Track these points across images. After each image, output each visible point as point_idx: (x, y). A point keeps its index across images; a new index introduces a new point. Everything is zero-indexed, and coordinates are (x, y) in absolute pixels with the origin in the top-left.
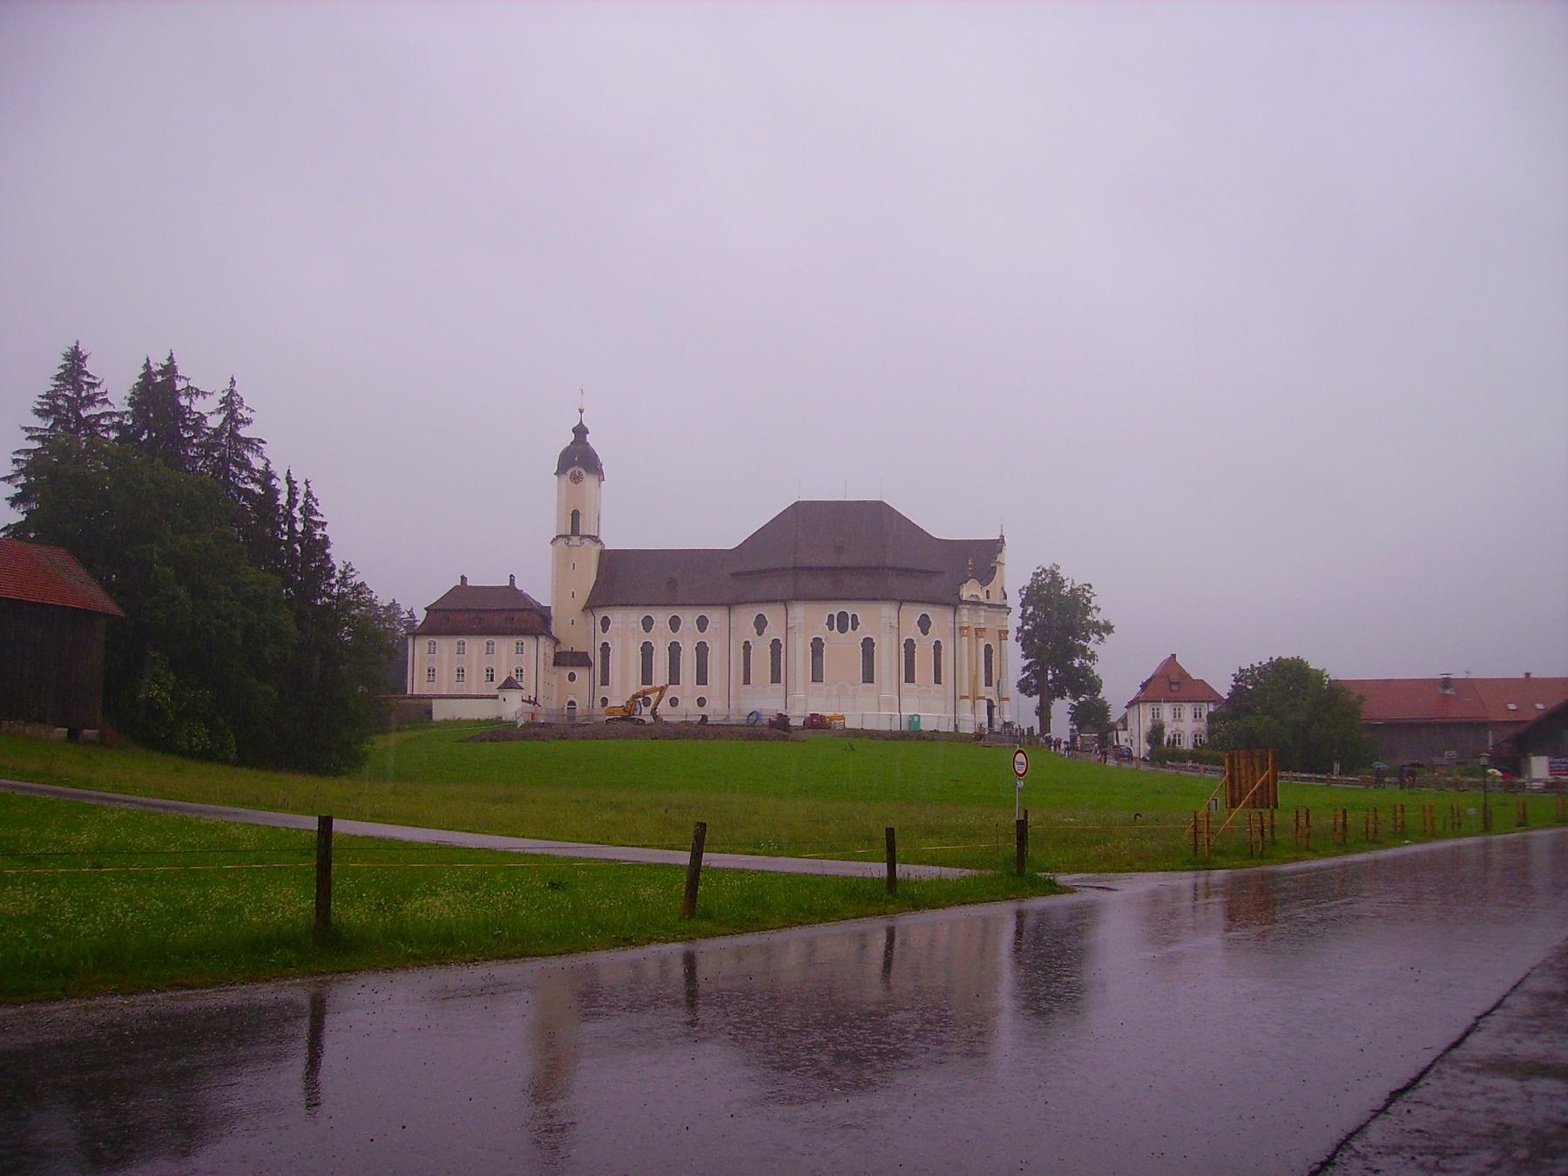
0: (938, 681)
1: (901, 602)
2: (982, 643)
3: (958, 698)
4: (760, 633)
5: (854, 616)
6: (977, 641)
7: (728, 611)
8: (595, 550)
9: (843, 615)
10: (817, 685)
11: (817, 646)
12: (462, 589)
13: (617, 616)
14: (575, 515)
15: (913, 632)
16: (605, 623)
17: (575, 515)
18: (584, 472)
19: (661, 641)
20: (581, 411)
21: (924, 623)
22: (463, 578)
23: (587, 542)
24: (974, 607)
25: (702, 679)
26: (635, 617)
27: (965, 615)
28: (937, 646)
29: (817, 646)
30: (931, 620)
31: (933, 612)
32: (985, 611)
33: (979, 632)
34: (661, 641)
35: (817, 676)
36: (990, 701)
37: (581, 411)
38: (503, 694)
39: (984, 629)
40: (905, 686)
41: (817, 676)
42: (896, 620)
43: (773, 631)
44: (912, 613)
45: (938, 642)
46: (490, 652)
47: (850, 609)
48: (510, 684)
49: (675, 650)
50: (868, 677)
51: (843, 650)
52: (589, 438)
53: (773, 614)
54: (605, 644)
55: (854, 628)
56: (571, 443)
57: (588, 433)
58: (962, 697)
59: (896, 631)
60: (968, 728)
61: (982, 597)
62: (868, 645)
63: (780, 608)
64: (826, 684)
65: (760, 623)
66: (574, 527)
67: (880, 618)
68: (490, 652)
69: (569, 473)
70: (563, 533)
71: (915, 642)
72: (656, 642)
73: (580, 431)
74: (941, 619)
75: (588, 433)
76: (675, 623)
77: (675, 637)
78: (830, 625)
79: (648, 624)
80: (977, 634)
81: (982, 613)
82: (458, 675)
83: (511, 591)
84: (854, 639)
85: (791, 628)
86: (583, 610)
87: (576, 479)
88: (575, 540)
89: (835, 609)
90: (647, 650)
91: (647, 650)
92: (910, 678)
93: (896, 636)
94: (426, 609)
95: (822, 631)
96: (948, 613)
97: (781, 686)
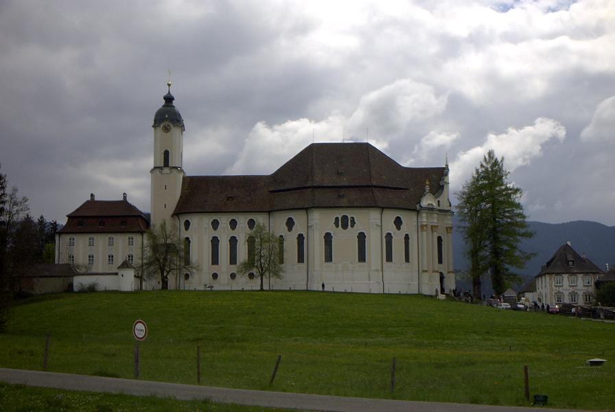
0: (407, 260)
1: (383, 208)
2: (436, 235)
3: (421, 271)
4: (290, 229)
6: (432, 235)
7: (268, 219)
8: (181, 176)
9: (345, 218)
11: (328, 238)
12: (92, 203)
13: (195, 220)
14: (166, 154)
15: (390, 227)
16: (187, 224)
17: (166, 154)
18: (172, 126)
19: (224, 235)
20: (169, 85)
21: (398, 222)
22: (92, 195)
23: (174, 171)
24: (430, 212)
26: (206, 220)
27: (424, 218)
28: (407, 237)
29: (328, 238)
30: (402, 220)
31: (404, 216)
32: (438, 214)
33: (433, 228)
34: (224, 235)
35: (329, 258)
36: (441, 274)
38: (121, 272)
39: (437, 226)
40: (386, 264)
41: (329, 258)
43: (299, 228)
44: (390, 216)
45: (407, 235)
46: (111, 244)
47: (350, 214)
48: (125, 265)
49: (233, 241)
50: (362, 258)
51: (345, 241)
53: (299, 218)
54: (187, 239)
55: (352, 226)
56: (163, 106)
57: (173, 99)
58: (424, 271)
59: (379, 228)
60: (426, 290)
61: (435, 205)
62: (362, 237)
63: (303, 212)
65: (290, 224)
66: (166, 161)
67: (369, 219)
68: (111, 244)
69: (162, 126)
70: (158, 165)
71: (392, 235)
72: (238, 236)
73: (169, 99)
74: (409, 220)
75: (173, 99)
76: (233, 224)
77: (233, 233)
79: (215, 224)
80: (432, 229)
81: (435, 216)
82: (90, 260)
83: (124, 204)
84: (351, 235)
85: (311, 226)
86: (172, 216)
87: (167, 129)
88: (166, 170)
89: (340, 214)
90: (215, 242)
91: (215, 242)
92: (389, 258)
93: (379, 231)
94: (67, 216)
95: (331, 228)
96: (413, 216)
97: (304, 265)
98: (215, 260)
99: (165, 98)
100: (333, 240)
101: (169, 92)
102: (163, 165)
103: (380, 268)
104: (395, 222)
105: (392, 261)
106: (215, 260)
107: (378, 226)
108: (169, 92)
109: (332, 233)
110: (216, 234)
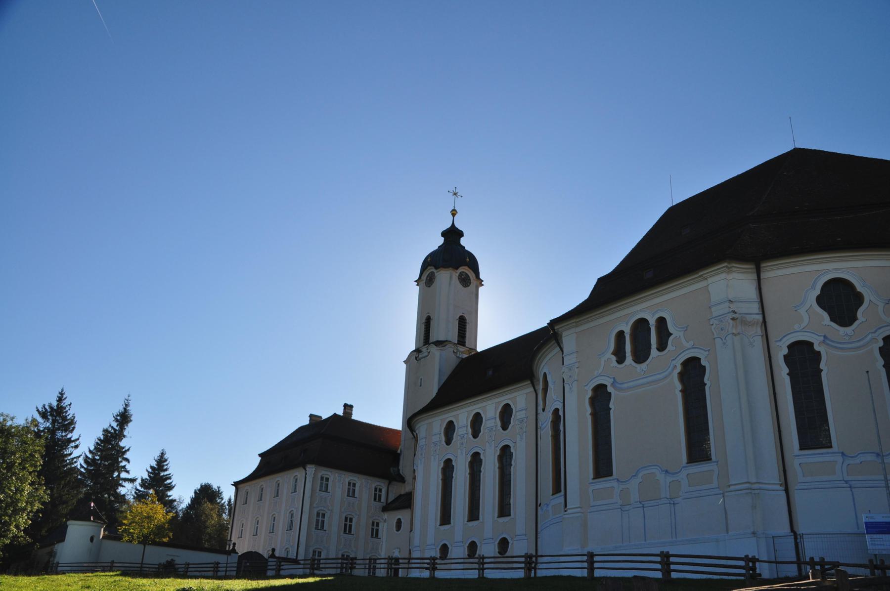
5: (661, 322)
10: (604, 484)
20: (454, 213)
23: (434, 349)
25: (504, 510)
37: (454, 213)
52: (463, 241)
55: (662, 347)
57: (461, 234)
59: (759, 330)
64: (618, 480)
73: (452, 235)
77: (476, 445)
93: (759, 342)
98: (446, 518)
99: (444, 234)
100: (611, 406)
103: (772, 474)
104: (821, 301)
106: (446, 518)
107: (744, 323)
109: (607, 381)
110: (448, 452)
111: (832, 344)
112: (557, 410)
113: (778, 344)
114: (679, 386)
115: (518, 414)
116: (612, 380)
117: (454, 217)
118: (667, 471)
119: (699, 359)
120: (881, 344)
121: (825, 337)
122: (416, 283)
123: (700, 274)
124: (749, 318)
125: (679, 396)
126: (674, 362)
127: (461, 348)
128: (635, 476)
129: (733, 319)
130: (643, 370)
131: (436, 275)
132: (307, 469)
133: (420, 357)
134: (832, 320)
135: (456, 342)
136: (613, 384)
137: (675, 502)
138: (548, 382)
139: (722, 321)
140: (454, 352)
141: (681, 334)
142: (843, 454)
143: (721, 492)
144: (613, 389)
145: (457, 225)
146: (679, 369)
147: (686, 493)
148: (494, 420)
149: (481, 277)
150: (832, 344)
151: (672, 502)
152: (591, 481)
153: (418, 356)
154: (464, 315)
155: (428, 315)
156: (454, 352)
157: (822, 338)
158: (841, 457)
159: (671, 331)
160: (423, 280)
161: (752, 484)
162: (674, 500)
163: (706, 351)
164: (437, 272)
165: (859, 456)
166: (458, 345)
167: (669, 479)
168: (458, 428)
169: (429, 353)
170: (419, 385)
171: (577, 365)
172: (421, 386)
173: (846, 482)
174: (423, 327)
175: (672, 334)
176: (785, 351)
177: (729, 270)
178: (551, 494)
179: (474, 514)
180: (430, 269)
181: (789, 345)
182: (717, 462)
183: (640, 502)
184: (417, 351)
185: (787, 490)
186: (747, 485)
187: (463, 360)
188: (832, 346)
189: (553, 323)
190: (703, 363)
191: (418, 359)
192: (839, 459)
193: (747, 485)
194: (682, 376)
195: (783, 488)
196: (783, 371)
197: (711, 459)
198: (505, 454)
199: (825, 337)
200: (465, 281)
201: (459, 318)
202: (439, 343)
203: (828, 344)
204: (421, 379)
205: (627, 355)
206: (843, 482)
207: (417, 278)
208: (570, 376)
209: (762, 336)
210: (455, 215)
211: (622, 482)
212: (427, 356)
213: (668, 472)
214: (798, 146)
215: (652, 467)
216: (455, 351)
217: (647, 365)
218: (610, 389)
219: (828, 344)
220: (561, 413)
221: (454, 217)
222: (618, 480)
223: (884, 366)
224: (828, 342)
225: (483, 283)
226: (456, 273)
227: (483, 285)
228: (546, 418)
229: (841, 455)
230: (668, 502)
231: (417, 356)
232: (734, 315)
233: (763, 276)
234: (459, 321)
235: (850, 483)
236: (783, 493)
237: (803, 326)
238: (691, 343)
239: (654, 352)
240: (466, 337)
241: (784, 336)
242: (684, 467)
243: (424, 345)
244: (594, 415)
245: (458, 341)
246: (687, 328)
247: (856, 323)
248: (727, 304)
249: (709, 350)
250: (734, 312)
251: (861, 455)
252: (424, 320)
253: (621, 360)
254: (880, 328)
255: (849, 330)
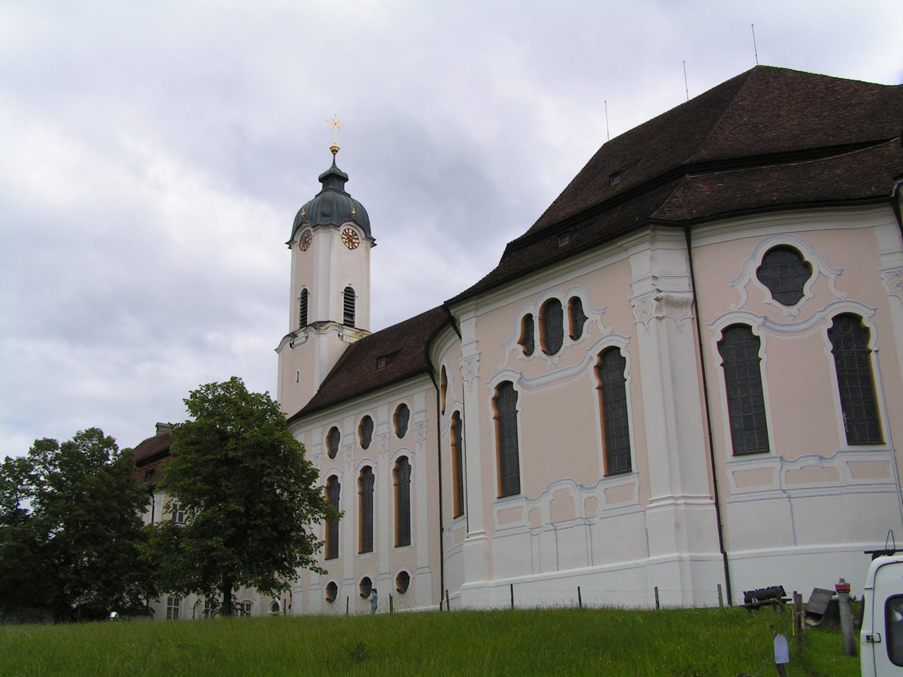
5: (576, 302)
10: (511, 503)
20: (334, 151)
25: (403, 537)
30: (807, 257)
37: (334, 151)
42: (686, 283)
55: (576, 334)
57: (347, 180)
59: (689, 312)
64: (526, 498)
78: (527, 342)
87: (305, 243)
93: (689, 327)
99: (324, 179)
101: (334, 163)
102: (298, 326)
105: (766, 450)
108: (334, 163)
111: (773, 326)
112: (457, 414)
113: (711, 328)
114: (595, 382)
115: (416, 416)
116: (519, 376)
117: (334, 155)
118: (582, 486)
119: (618, 349)
120: (830, 324)
121: (765, 318)
122: (288, 246)
123: (619, 244)
124: (677, 296)
125: (596, 394)
126: (590, 352)
127: (348, 332)
128: (546, 492)
129: (657, 299)
130: (554, 363)
131: (312, 235)
132: (154, 496)
133: (295, 343)
134: (773, 298)
135: (342, 323)
136: (519, 381)
137: (591, 523)
138: (446, 376)
139: (644, 301)
140: (339, 335)
141: (598, 318)
142: (781, 458)
143: (642, 509)
144: (520, 387)
145: (338, 166)
146: (596, 361)
147: (547, 524)
148: (386, 426)
149: (373, 235)
150: (773, 326)
151: (588, 523)
152: (496, 500)
153: (293, 343)
154: (351, 286)
155: (304, 288)
156: (339, 335)
157: (762, 320)
158: (780, 463)
159: (586, 313)
160: (296, 242)
161: (677, 498)
162: (590, 520)
163: (626, 339)
164: (314, 231)
165: (799, 461)
166: (344, 327)
167: (585, 495)
168: (344, 436)
169: (307, 337)
170: (296, 381)
171: (477, 357)
172: (298, 382)
173: (784, 491)
174: (299, 304)
175: (588, 318)
176: (719, 337)
177: (653, 240)
178: (453, 516)
179: (366, 544)
180: (305, 227)
181: (723, 330)
182: (638, 473)
183: (552, 524)
184: (293, 335)
185: (717, 504)
186: (671, 501)
187: (351, 345)
188: (772, 329)
189: (450, 304)
190: (623, 353)
191: (293, 346)
192: (777, 464)
193: (671, 501)
194: (600, 369)
195: (713, 501)
196: (715, 360)
197: (631, 471)
198: (402, 466)
199: (765, 318)
200: (350, 241)
201: (345, 290)
202: (318, 325)
203: (768, 328)
204: (298, 372)
205: (536, 344)
206: (782, 492)
207: (288, 239)
208: (470, 372)
209: (693, 319)
210: (337, 151)
211: (531, 500)
212: (304, 343)
213: (584, 488)
214: (761, 63)
215: (565, 482)
216: (341, 334)
217: (559, 357)
218: (516, 387)
219: (768, 328)
220: (461, 417)
221: (334, 155)
222: (526, 498)
223: (832, 352)
224: (768, 324)
225: (375, 242)
226: (339, 230)
227: (376, 245)
228: (447, 421)
229: (779, 459)
230: (583, 522)
231: (292, 342)
232: (659, 295)
233: (694, 244)
234: (345, 294)
235: (789, 492)
236: (714, 507)
237: (740, 306)
238: (610, 329)
239: (567, 340)
240: (354, 315)
241: (718, 319)
242: (600, 481)
243: (301, 328)
244: (498, 418)
245: (344, 320)
246: (604, 310)
247: (802, 301)
248: (651, 281)
249: (630, 338)
250: (661, 292)
251: (802, 459)
252: (299, 296)
253: (529, 352)
254: (829, 306)
255: (793, 309)
